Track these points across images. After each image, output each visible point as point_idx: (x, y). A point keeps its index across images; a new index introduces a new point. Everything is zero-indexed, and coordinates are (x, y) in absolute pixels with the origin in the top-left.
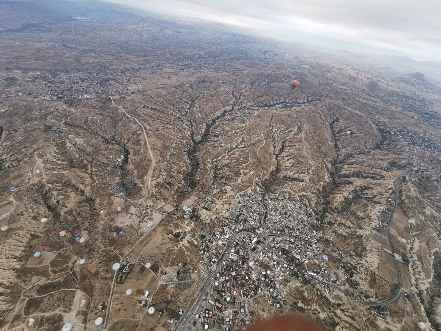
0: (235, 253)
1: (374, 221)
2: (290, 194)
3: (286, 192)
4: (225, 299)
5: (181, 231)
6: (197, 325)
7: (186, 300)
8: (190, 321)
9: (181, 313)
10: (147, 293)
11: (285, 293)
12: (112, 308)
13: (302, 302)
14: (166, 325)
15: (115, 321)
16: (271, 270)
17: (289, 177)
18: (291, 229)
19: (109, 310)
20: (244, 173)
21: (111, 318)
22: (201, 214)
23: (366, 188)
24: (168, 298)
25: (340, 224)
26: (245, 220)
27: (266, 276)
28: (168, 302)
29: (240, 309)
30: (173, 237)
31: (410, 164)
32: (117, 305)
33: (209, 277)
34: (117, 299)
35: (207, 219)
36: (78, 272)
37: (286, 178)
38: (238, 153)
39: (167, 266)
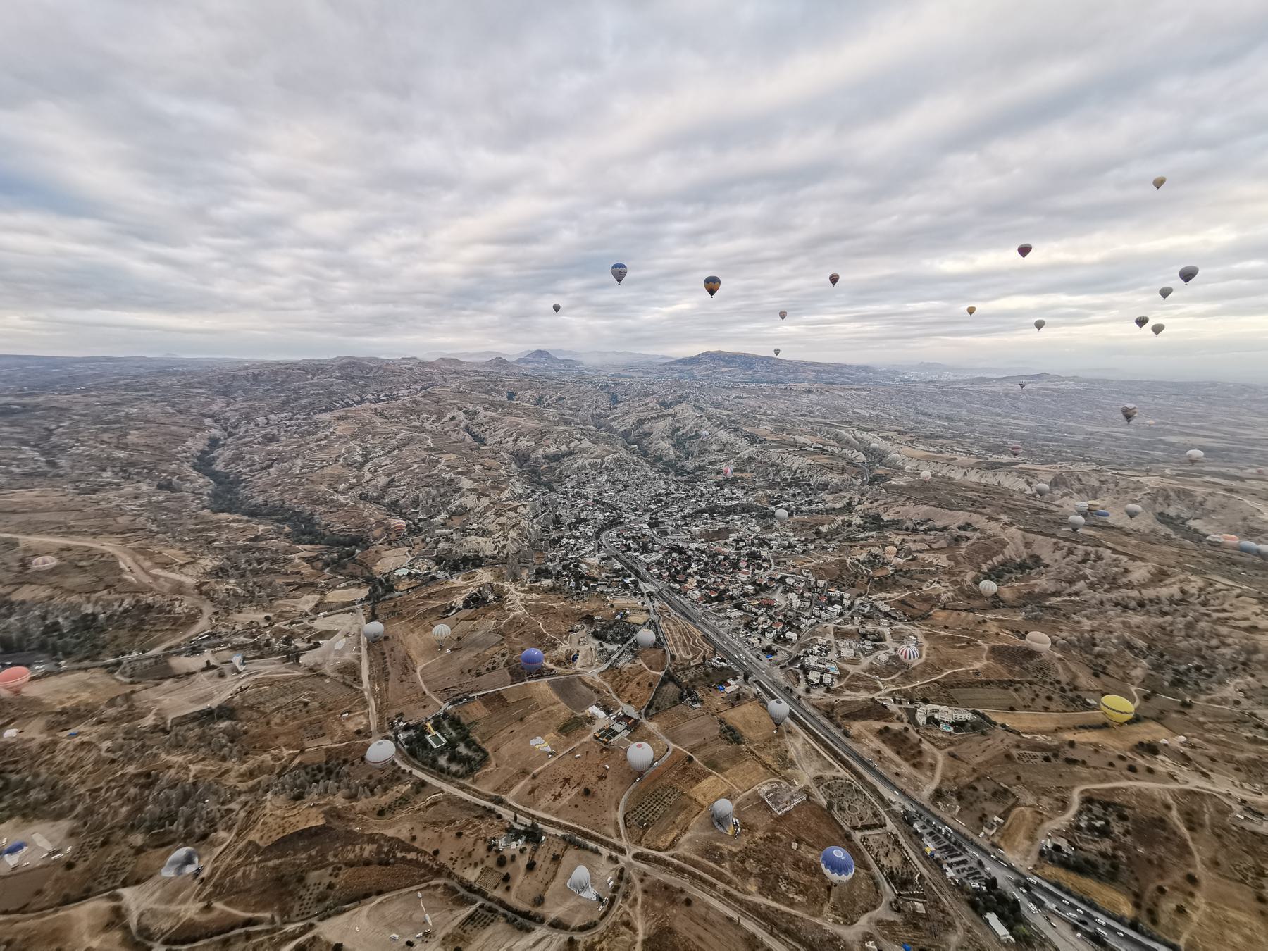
0: (642, 554)
1: (738, 442)
2: (593, 466)
3: (584, 467)
4: (746, 595)
5: (473, 590)
6: (773, 648)
7: (692, 649)
8: (758, 657)
9: (724, 664)
10: (594, 710)
11: (792, 534)
12: (557, 814)
13: (823, 525)
14: (738, 698)
15: (619, 816)
16: (732, 531)
17: (554, 456)
18: (667, 494)
19: (558, 826)
20: (461, 473)
21: (597, 826)
22: (475, 546)
23: (676, 430)
24: (655, 676)
25: (711, 463)
26: (579, 520)
27: (737, 541)
28: (669, 678)
29: (784, 583)
30: (468, 612)
31: (680, 397)
32: (557, 797)
33: (664, 598)
34: (532, 791)
35: (504, 546)
36: (208, 908)
37: (557, 458)
38: (388, 462)
39: (554, 645)
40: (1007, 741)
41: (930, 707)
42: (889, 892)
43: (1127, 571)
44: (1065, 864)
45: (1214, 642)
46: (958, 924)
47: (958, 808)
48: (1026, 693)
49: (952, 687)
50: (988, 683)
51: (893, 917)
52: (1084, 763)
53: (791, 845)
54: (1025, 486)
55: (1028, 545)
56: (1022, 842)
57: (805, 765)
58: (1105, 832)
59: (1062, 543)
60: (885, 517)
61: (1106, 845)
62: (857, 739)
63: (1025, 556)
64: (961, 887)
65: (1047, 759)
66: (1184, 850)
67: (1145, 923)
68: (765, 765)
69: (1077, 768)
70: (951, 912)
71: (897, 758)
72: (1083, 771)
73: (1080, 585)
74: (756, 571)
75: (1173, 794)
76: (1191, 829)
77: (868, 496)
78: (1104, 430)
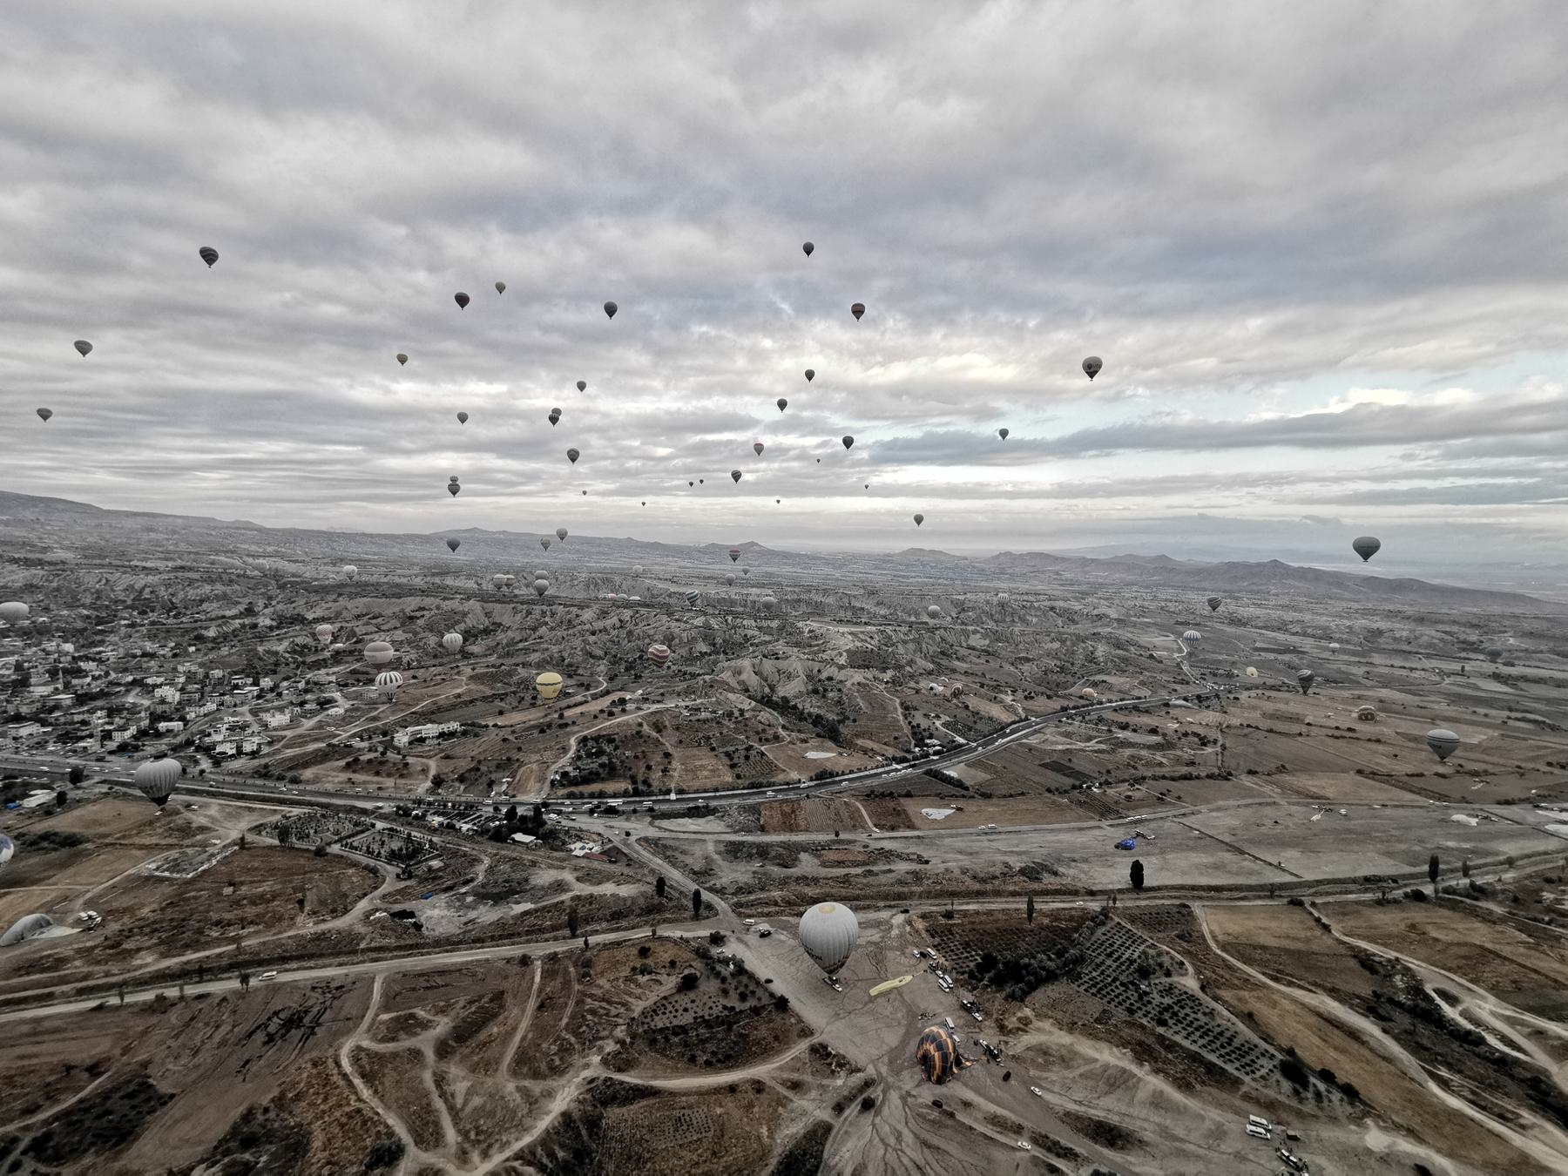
40: (501, 734)
41: (410, 729)
42: (391, 870)
43: (578, 616)
44: (574, 782)
45: (647, 641)
46: (482, 856)
47: (462, 787)
48: (512, 700)
49: (433, 713)
50: (471, 702)
51: (403, 884)
52: (574, 723)
53: (220, 894)
54: (475, 586)
55: (488, 615)
56: (533, 784)
57: (229, 825)
58: (600, 753)
59: (520, 607)
60: (310, 616)
61: (604, 759)
62: (316, 780)
63: (487, 623)
64: (483, 832)
65: (542, 731)
66: (657, 743)
67: (641, 787)
68: (142, 847)
69: (568, 729)
70: (474, 852)
71: (376, 779)
72: (575, 728)
73: (543, 630)
74: (75, 682)
75: (643, 717)
76: (659, 731)
77: (279, 599)
78: (538, 561)
